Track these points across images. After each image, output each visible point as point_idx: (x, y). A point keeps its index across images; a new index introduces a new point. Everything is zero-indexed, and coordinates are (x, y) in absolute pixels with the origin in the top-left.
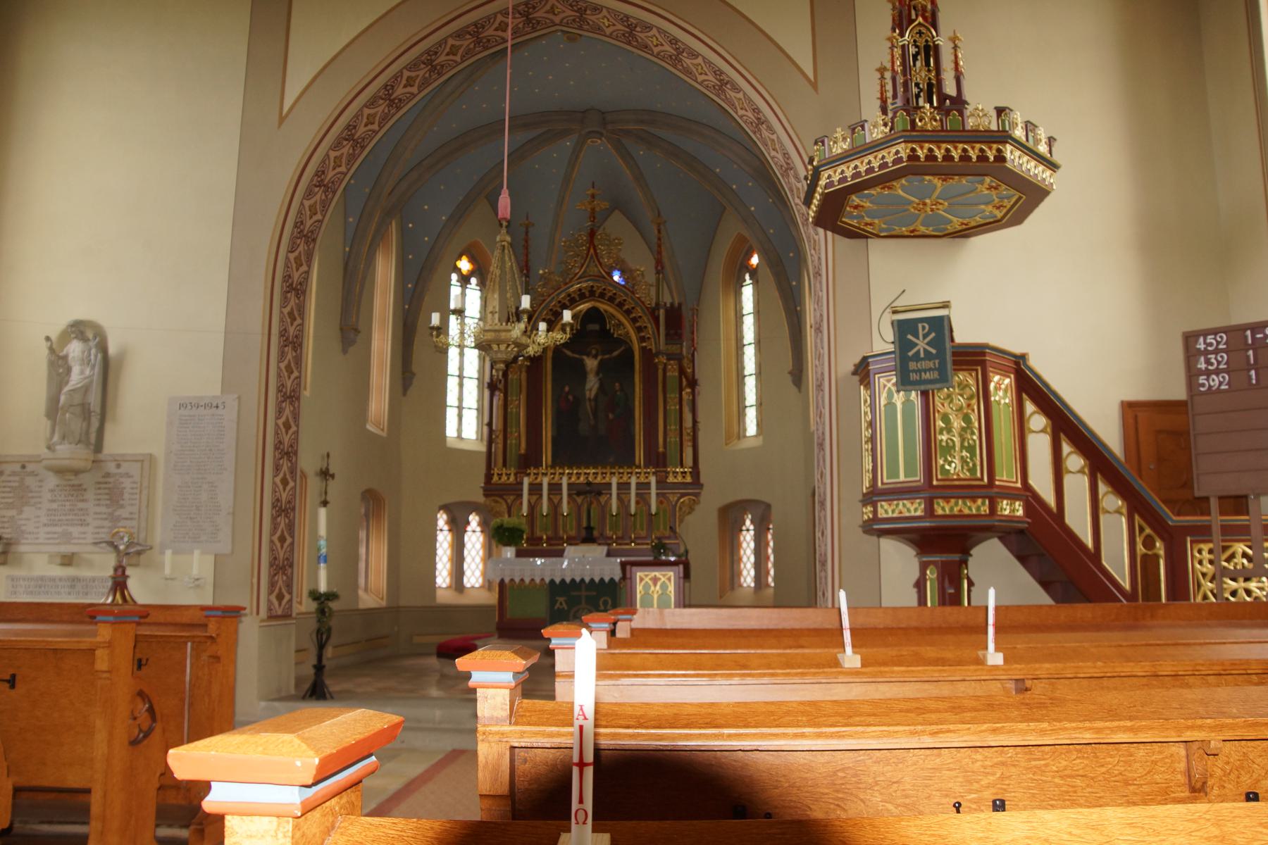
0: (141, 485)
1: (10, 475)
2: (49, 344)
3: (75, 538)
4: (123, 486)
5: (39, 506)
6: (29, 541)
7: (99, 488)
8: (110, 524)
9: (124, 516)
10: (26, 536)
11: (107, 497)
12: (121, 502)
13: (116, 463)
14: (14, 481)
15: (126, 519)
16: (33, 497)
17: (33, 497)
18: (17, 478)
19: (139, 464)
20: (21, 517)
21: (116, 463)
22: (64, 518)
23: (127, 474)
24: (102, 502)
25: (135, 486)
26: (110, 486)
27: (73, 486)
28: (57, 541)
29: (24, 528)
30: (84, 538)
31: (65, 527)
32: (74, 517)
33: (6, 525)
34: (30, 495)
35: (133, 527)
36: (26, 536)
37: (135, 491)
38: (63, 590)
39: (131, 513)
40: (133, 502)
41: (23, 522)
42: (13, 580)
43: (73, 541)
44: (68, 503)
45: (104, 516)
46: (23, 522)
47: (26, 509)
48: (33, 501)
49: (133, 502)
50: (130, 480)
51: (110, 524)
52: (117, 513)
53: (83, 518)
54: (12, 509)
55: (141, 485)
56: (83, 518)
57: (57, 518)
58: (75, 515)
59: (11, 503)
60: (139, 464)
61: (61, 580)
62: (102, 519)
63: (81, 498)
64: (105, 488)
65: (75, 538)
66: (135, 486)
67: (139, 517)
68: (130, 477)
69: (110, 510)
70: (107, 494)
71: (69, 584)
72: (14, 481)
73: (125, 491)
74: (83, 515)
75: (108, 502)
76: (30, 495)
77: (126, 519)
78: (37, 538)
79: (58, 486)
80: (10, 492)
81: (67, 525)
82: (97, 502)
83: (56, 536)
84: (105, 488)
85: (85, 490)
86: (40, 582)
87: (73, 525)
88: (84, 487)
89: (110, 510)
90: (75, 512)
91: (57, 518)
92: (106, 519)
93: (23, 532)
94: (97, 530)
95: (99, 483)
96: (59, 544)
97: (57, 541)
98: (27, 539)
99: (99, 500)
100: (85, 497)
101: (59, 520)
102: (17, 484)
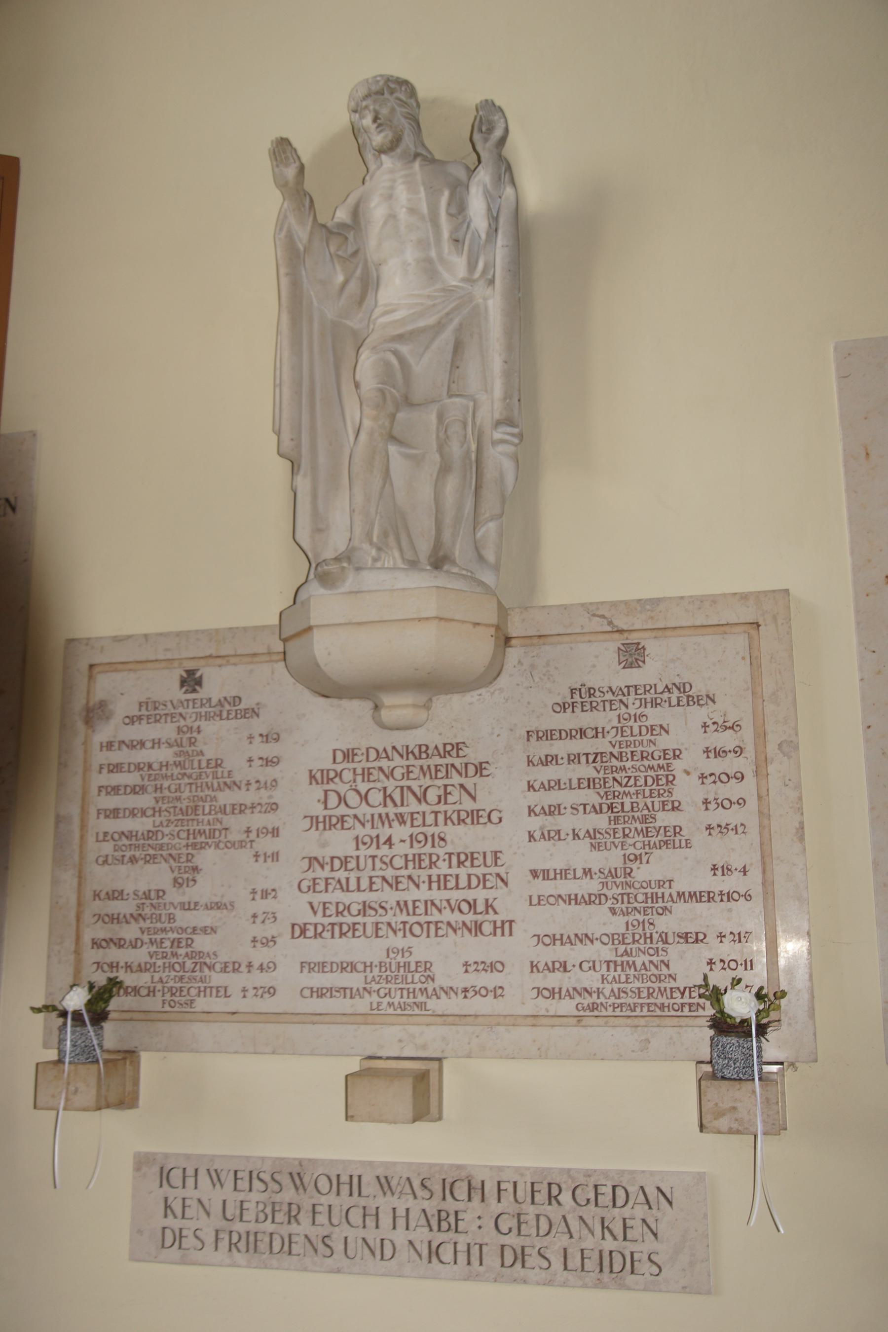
0: (761, 735)
1: (132, 720)
2: (290, 172)
3: (449, 991)
4: (665, 742)
5: (266, 844)
6: (236, 1003)
7: (549, 760)
8: (617, 924)
9: (678, 887)
10: (217, 979)
11: (591, 797)
12: (664, 819)
13: (617, 642)
14: (156, 743)
15: (695, 897)
16: (240, 809)
17: (240, 809)
18: (167, 731)
19: (738, 642)
20: (191, 894)
21: (617, 642)
22: (390, 897)
23: (681, 688)
24: (565, 822)
25: (727, 740)
26: (602, 745)
27: (423, 750)
28: (362, 1005)
29: (202, 943)
30: (497, 992)
31: (398, 941)
32: (437, 895)
33: (130, 932)
34: (226, 798)
35: (739, 938)
36: (217, 979)
37: (731, 764)
38: (400, 1237)
39: (720, 870)
40: (732, 816)
41: (204, 918)
42: (165, 1176)
43: (432, 1004)
44: (400, 832)
45: (592, 886)
46: (204, 918)
47: (208, 858)
48: (236, 824)
49: (732, 816)
50: (699, 714)
51: (617, 924)
52: (642, 873)
53: (480, 895)
54: (150, 859)
55: (761, 735)
56: (480, 895)
57: (355, 898)
58: (442, 882)
59: (150, 834)
60: (738, 642)
61: (385, 1184)
62: (573, 899)
63: (468, 805)
64: (572, 759)
65: (449, 991)
66: (727, 740)
67: (767, 884)
68: (695, 701)
69: (613, 858)
70: (591, 783)
71: (431, 1207)
72: (156, 743)
73: (678, 766)
74: (483, 880)
75: (601, 822)
76: (226, 798)
77: (695, 897)
78: (272, 991)
79: (349, 755)
80: (135, 790)
81: (407, 929)
82: (536, 823)
83: (354, 980)
84: (572, 759)
85: (480, 769)
86: (289, 1194)
87: (432, 929)
88: (474, 755)
89: (613, 858)
90: (443, 868)
91: (355, 898)
92: (589, 900)
93: (202, 961)
94: (547, 955)
95: (549, 735)
96: (363, 1019)
97: (362, 1005)
98: (223, 992)
99: (554, 810)
100: (484, 802)
101: (365, 908)
102: (164, 754)
